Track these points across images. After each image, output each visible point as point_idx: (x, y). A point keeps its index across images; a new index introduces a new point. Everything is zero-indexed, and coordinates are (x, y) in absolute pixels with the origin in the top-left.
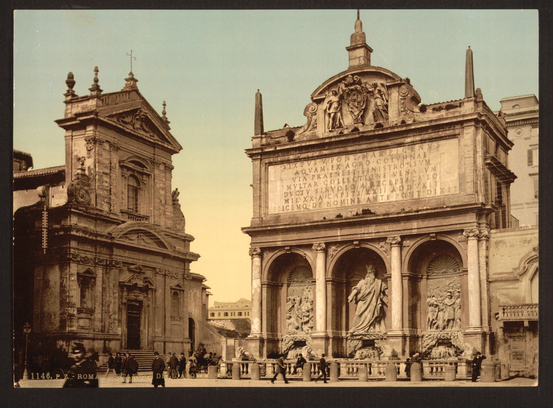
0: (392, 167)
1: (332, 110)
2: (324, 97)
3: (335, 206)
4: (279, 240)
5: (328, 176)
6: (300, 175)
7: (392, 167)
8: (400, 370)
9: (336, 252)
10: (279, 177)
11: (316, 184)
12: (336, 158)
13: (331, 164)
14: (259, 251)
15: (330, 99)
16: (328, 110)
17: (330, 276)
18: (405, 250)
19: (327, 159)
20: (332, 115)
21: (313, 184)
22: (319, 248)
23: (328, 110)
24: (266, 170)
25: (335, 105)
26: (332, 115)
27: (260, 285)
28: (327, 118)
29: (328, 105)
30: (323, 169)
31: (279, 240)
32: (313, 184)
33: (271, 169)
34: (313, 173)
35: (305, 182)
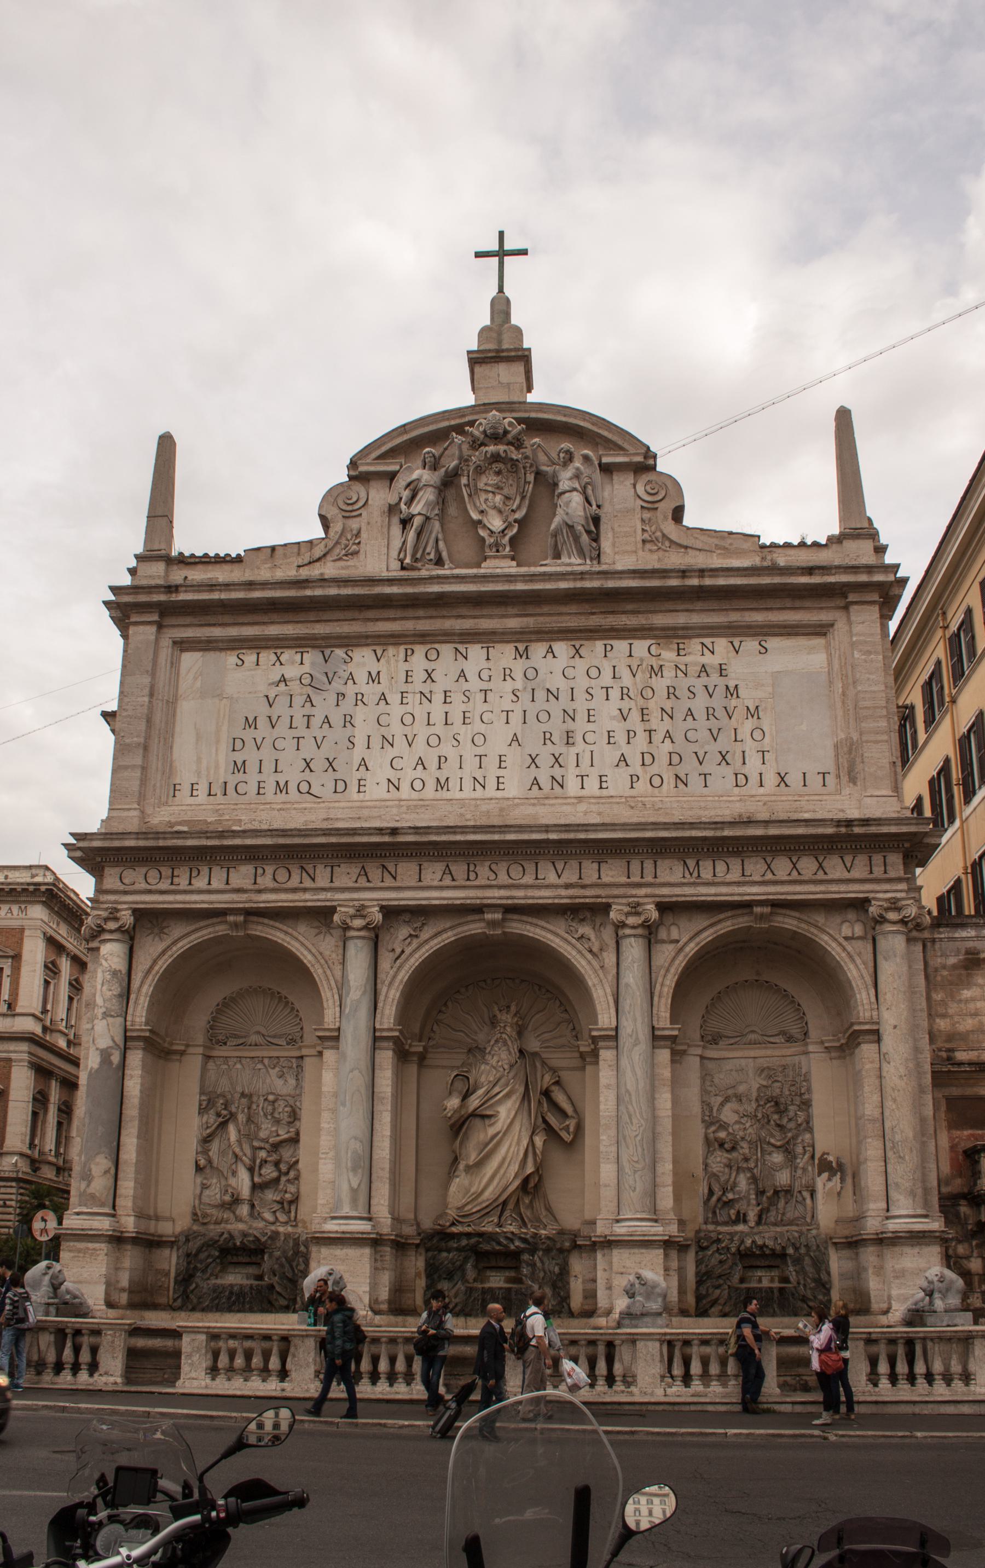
0: (615, 694)
1: (417, 508)
2: (397, 468)
3: (415, 795)
4: (207, 888)
5: (394, 698)
6: (295, 687)
7: (615, 694)
8: (206, 1363)
9: (415, 943)
10: (234, 683)
11: (348, 721)
12: (420, 650)
13: (403, 667)
14: (127, 918)
15: (415, 475)
16: (403, 507)
17: (388, 1017)
18: (664, 953)
19: (391, 651)
20: (417, 521)
21: (337, 720)
22: (358, 923)
23: (403, 507)
24: (175, 664)
25: (427, 496)
26: (417, 521)
27: (119, 1039)
28: (396, 529)
29: (406, 494)
30: (374, 678)
31: (207, 888)
32: (337, 720)
33: (189, 660)
34: (337, 685)
35: (308, 710)
